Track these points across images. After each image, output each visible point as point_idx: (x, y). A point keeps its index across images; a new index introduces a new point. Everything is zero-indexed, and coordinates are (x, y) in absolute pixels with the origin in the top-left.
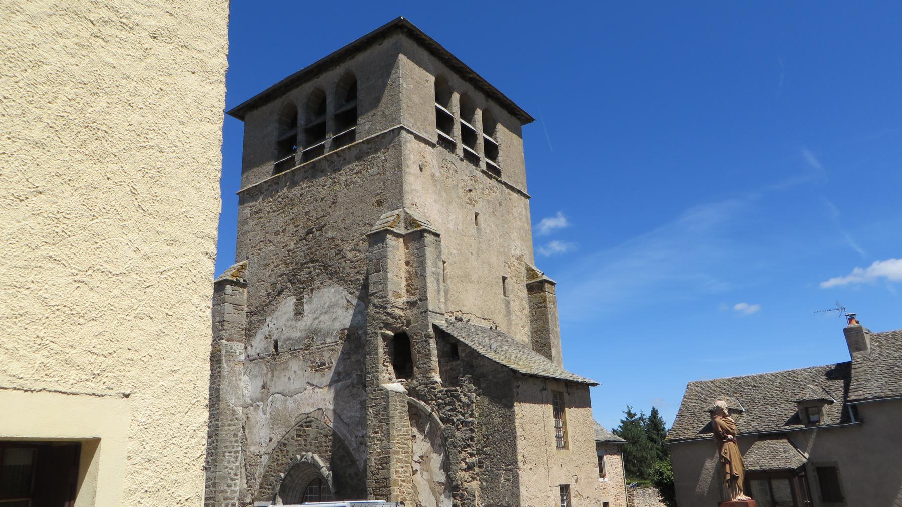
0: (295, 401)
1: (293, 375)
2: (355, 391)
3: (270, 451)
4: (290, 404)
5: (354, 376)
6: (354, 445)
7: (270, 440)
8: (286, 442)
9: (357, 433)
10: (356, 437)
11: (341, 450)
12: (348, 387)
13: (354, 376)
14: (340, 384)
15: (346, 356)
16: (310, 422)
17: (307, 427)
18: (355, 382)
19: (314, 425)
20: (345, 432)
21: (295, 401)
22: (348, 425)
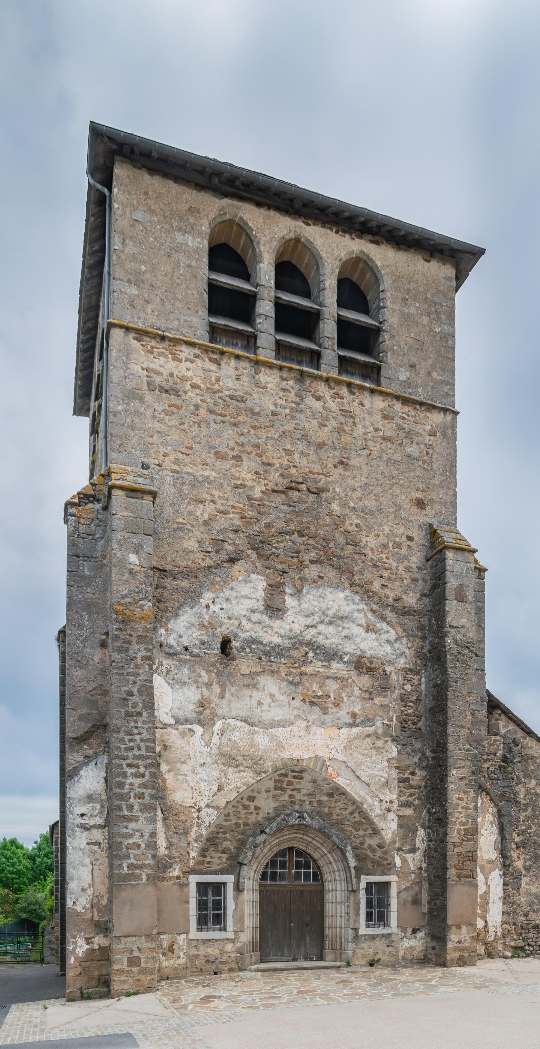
0: (273, 738)
1: (269, 700)
2: (380, 743)
3: (222, 803)
4: (262, 740)
5: (378, 724)
6: (378, 811)
7: (220, 789)
8: (255, 794)
9: (382, 797)
10: (381, 801)
11: (357, 815)
12: (369, 736)
13: (378, 724)
14: (355, 730)
15: (367, 696)
16: (301, 772)
17: (295, 777)
18: (380, 731)
19: (307, 777)
20: (363, 793)
21: (273, 738)
22: (368, 785)
